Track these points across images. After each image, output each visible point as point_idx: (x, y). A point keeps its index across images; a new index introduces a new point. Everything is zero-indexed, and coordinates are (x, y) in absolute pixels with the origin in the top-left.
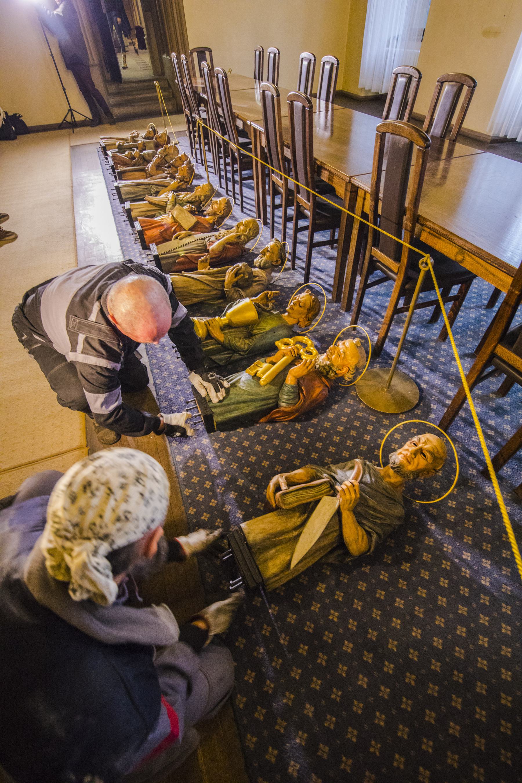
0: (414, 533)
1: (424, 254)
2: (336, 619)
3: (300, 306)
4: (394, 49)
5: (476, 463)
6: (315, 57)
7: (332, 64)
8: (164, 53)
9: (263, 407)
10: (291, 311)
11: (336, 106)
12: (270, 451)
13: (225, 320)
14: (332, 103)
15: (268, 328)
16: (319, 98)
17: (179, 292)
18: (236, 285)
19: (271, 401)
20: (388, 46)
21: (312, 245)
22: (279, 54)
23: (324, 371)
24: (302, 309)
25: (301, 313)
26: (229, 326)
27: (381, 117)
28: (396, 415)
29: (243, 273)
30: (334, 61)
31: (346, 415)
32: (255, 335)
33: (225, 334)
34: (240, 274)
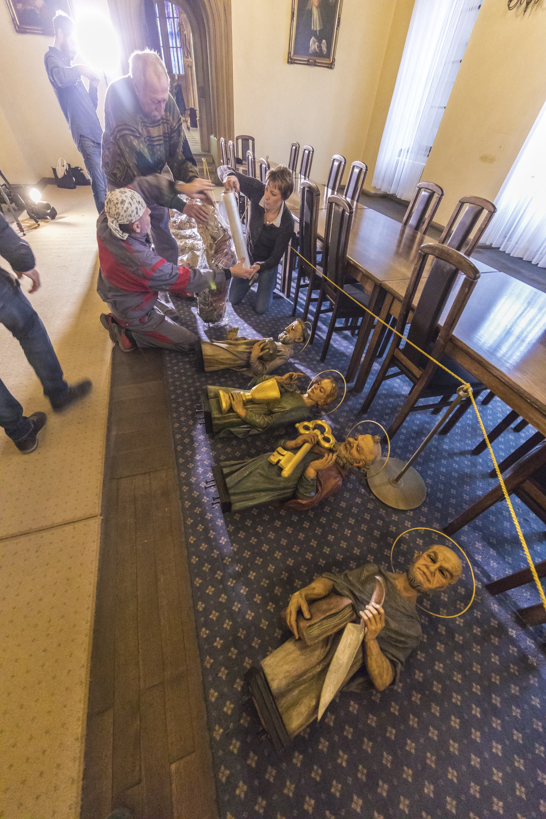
0: (424, 655)
1: (463, 382)
2: (344, 764)
3: (321, 391)
4: (404, 159)
5: (481, 575)
6: (345, 160)
7: (361, 169)
8: (212, 134)
9: (281, 497)
10: (311, 394)
11: (359, 205)
12: (283, 540)
13: (249, 396)
14: (357, 201)
15: (288, 407)
17: (208, 359)
18: (260, 358)
19: (289, 490)
20: (399, 156)
21: (332, 329)
23: (341, 463)
24: (322, 394)
25: (321, 398)
27: (401, 222)
28: (404, 511)
29: (269, 349)
30: (363, 166)
31: (357, 505)
32: (274, 413)
33: (247, 409)
34: (266, 349)
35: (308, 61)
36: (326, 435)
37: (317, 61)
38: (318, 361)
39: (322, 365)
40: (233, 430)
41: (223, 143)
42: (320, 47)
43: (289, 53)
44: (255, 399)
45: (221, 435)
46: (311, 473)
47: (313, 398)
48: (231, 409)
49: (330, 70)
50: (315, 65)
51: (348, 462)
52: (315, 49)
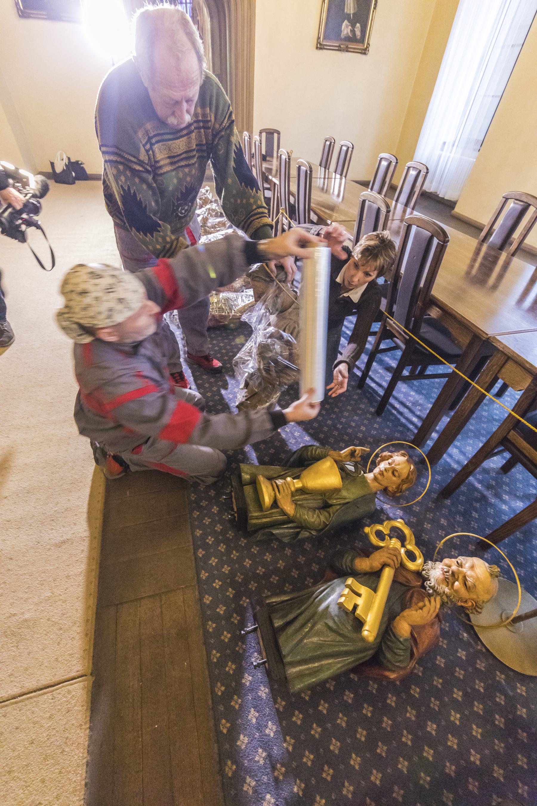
16: (397, 201)
22: (353, 148)
24: (394, 478)
26: (302, 491)
35: (339, 46)
36: (409, 547)
37: (349, 46)
38: (372, 414)
39: (379, 420)
40: (275, 532)
41: (246, 138)
42: (353, 31)
43: (319, 38)
44: (307, 489)
45: (259, 536)
46: (403, 628)
47: (382, 483)
48: (275, 504)
49: (364, 56)
50: (347, 51)
51: (451, 600)
52: (348, 33)
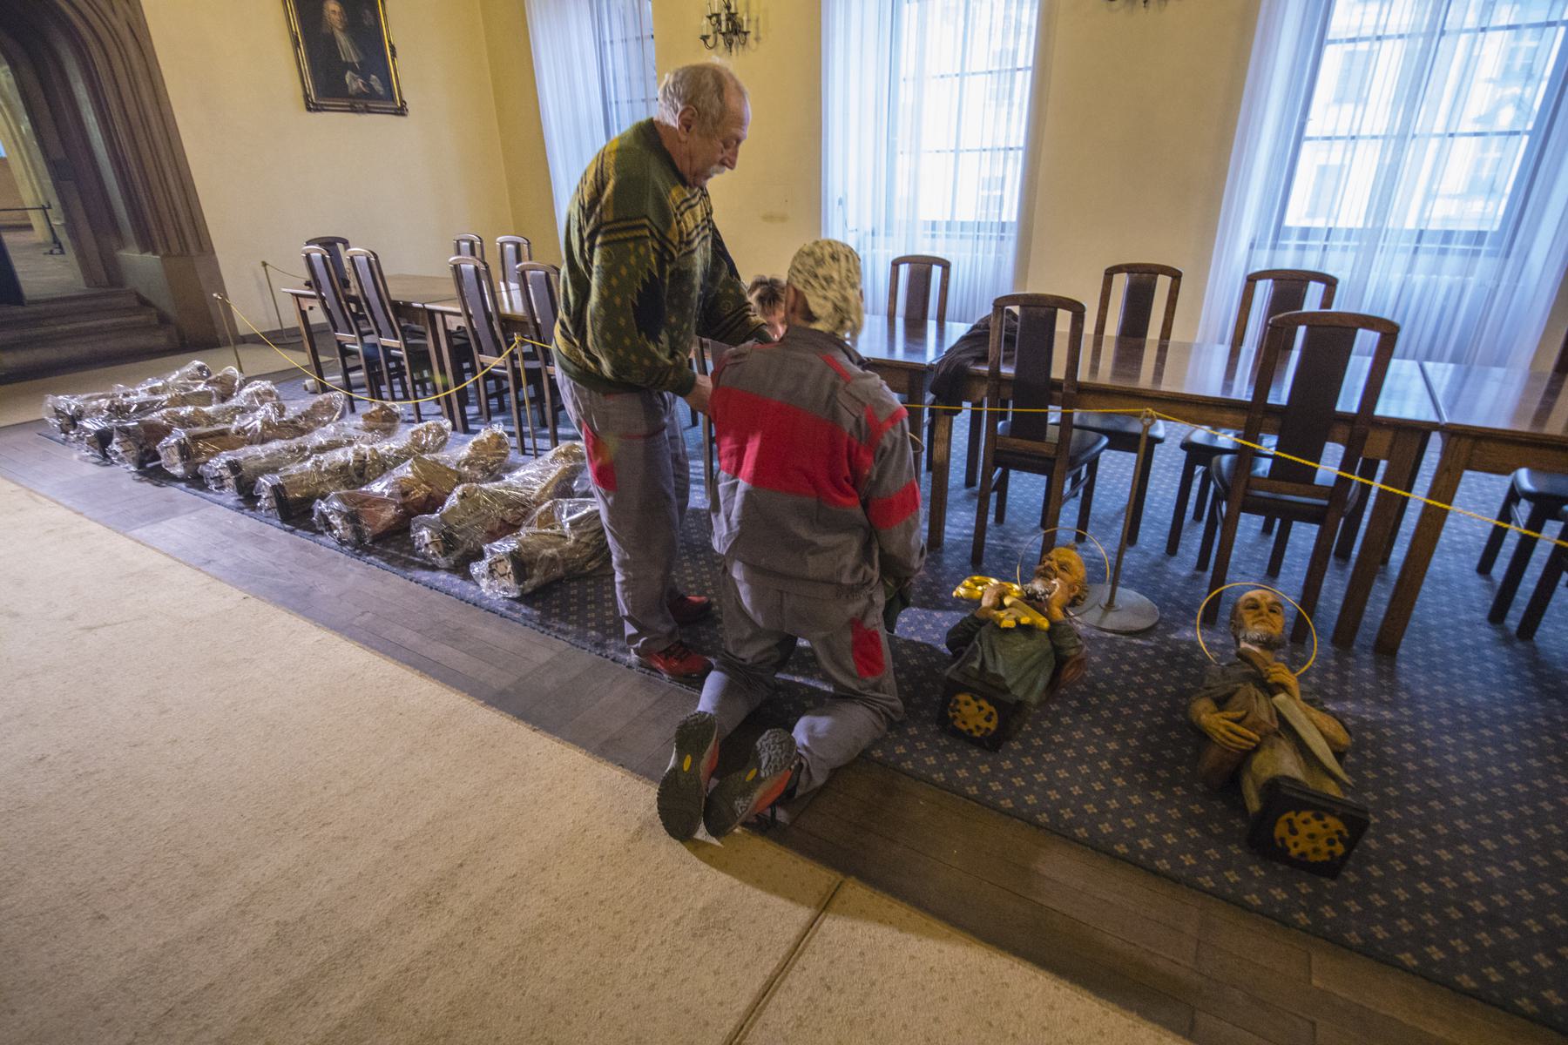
42: (367, 84)
43: (306, 96)
